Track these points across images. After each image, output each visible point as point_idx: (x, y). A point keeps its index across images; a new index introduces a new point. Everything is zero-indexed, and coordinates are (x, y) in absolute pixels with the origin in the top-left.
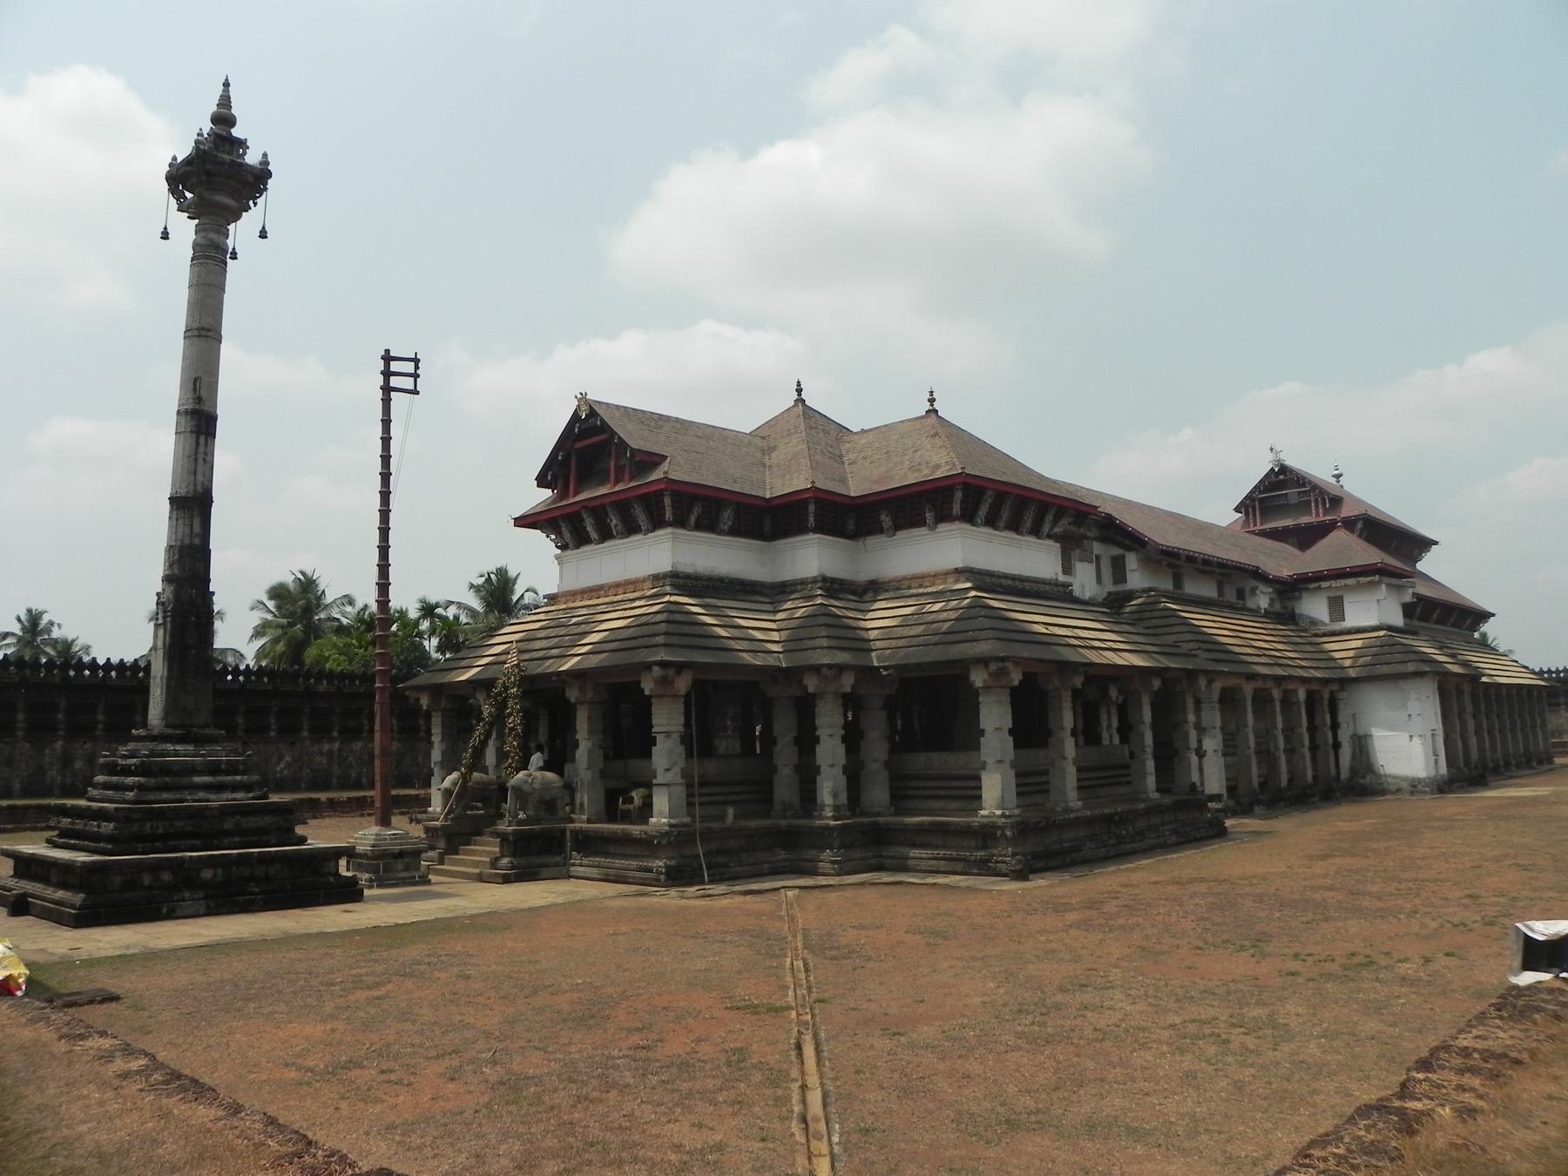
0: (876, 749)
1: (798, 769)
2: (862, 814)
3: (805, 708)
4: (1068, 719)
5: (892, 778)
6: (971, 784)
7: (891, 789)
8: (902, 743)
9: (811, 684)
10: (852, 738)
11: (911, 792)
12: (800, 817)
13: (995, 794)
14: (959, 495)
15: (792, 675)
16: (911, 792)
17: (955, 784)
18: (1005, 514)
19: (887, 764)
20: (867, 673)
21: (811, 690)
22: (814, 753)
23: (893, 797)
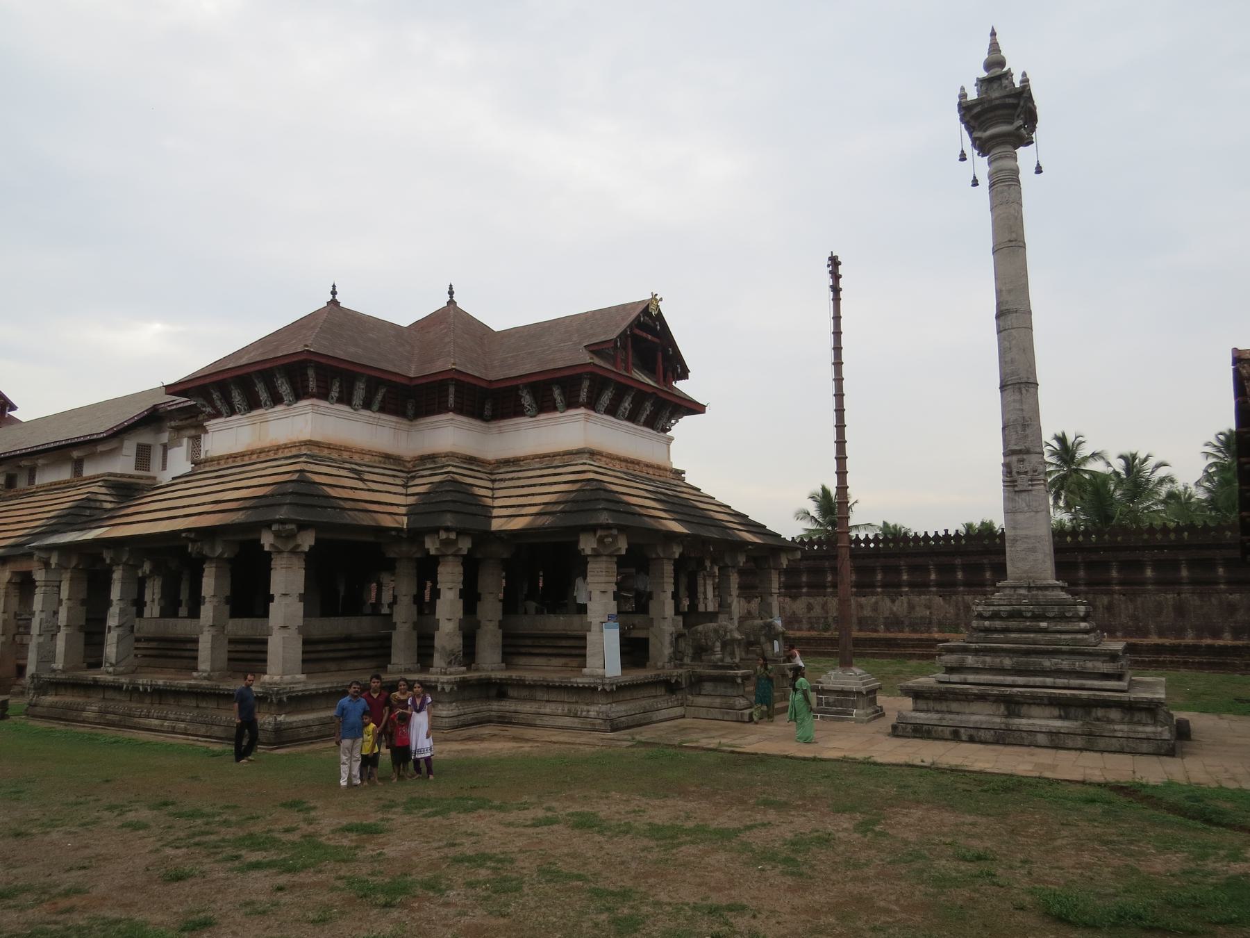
0: (491, 609)
1: (416, 626)
2: (477, 670)
3: (427, 569)
4: (670, 589)
5: (505, 636)
6: (576, 643)
7: (504, 646)
8: (510, 605)
9: (432, 546)
10: (470, 596)
11: (523, 650)
12: (415, 672)
13: (606, 654)
14: (586, 384)
15: (414, 535)
16: (523, 650)
17: (564, 643)
18: (627, 404)
19: (501, 625)
20: (484, 538)
21: (432, 552)
22: (434, 613)
23: (504, 653)
